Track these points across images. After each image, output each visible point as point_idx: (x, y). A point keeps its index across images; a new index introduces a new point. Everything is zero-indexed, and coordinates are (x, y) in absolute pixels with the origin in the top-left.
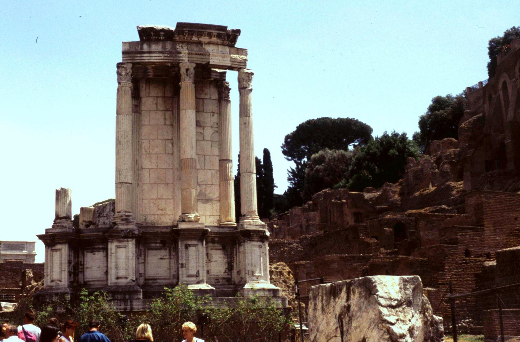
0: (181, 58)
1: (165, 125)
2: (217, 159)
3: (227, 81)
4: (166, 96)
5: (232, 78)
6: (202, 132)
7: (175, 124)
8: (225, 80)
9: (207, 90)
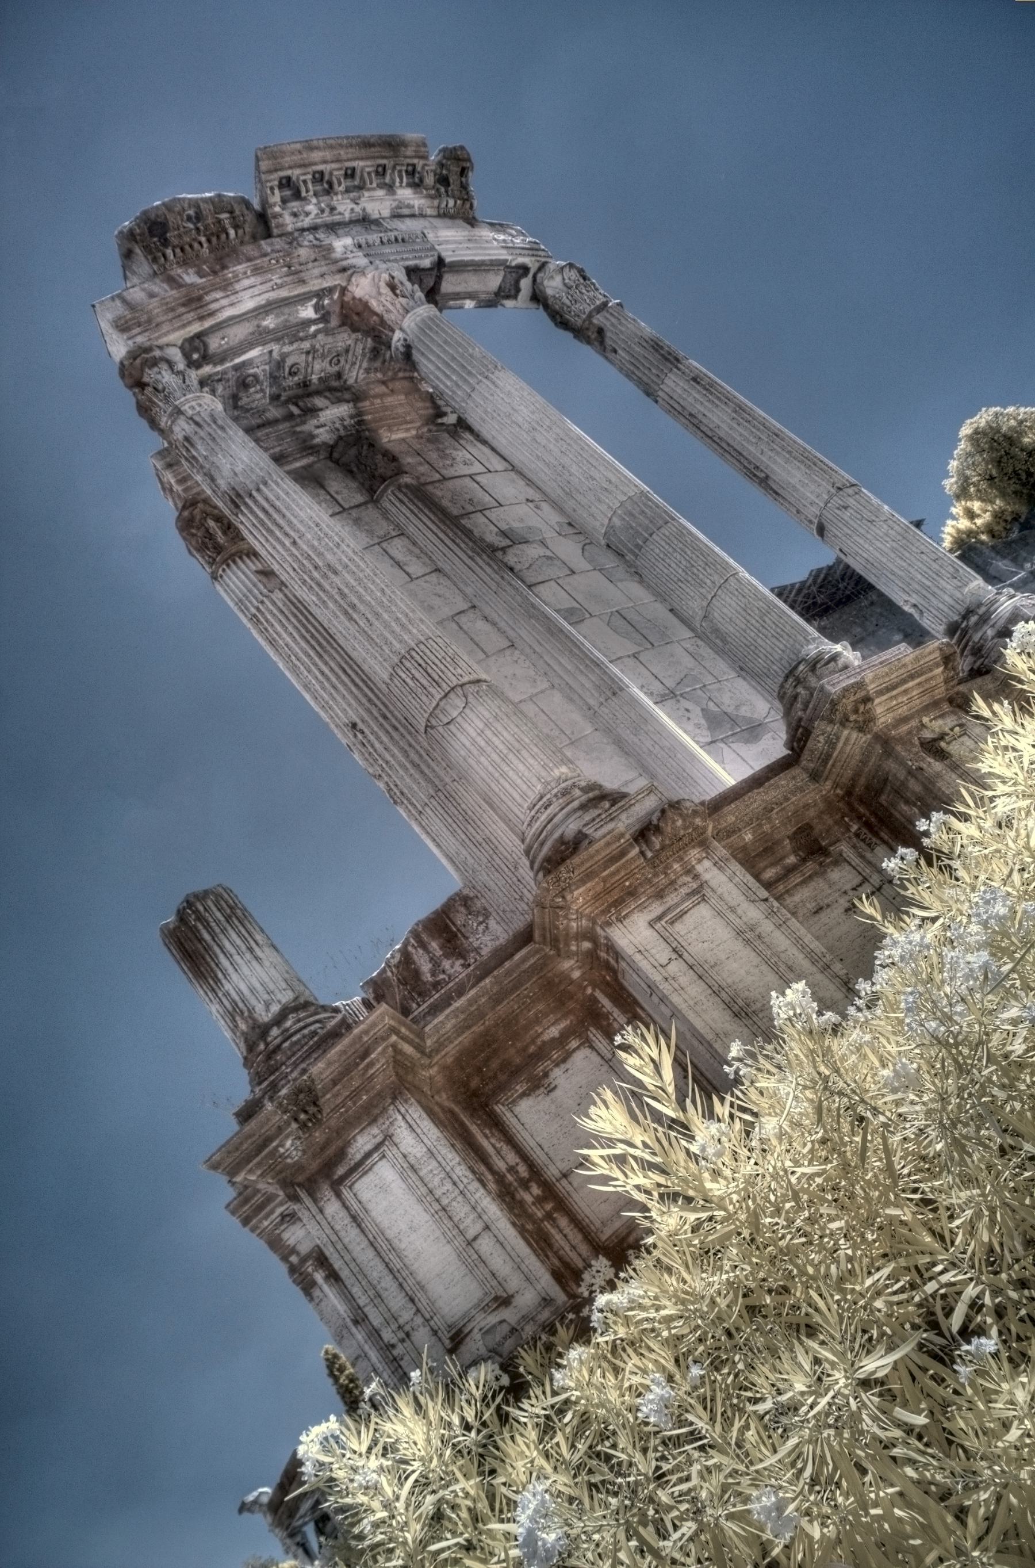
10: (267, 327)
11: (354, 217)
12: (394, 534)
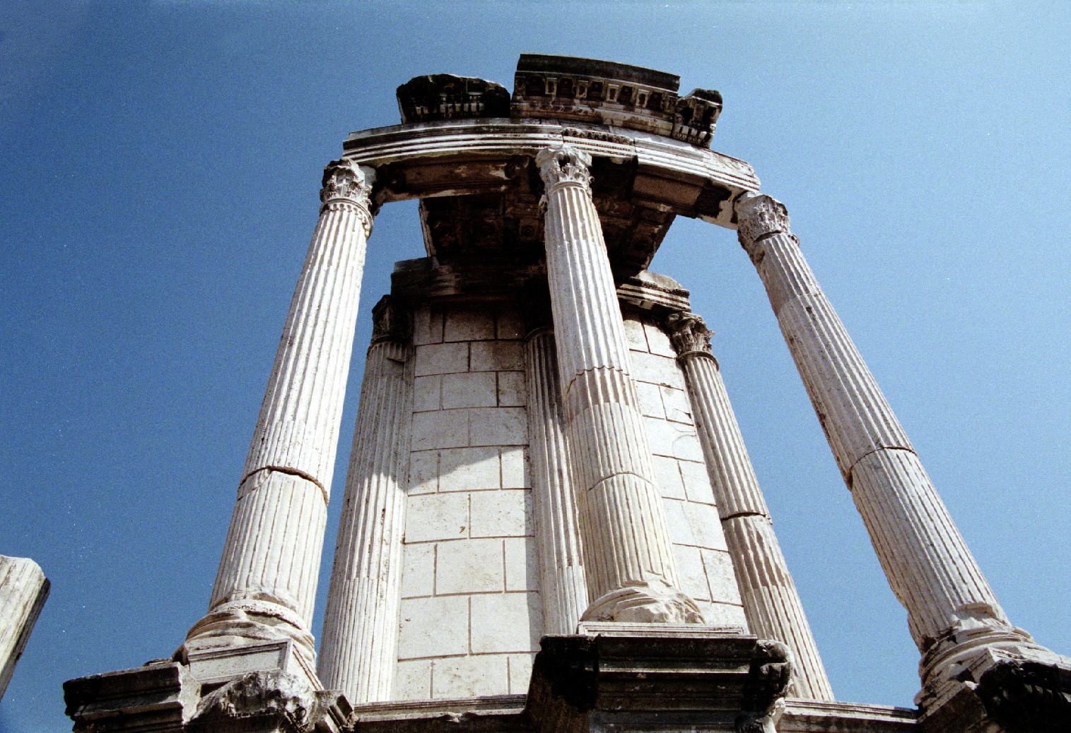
1: (498, 407)
2: (714, 514)
4: (499, 337)
10: (458, 176)
11: (587, 119)
12: (516, 368)
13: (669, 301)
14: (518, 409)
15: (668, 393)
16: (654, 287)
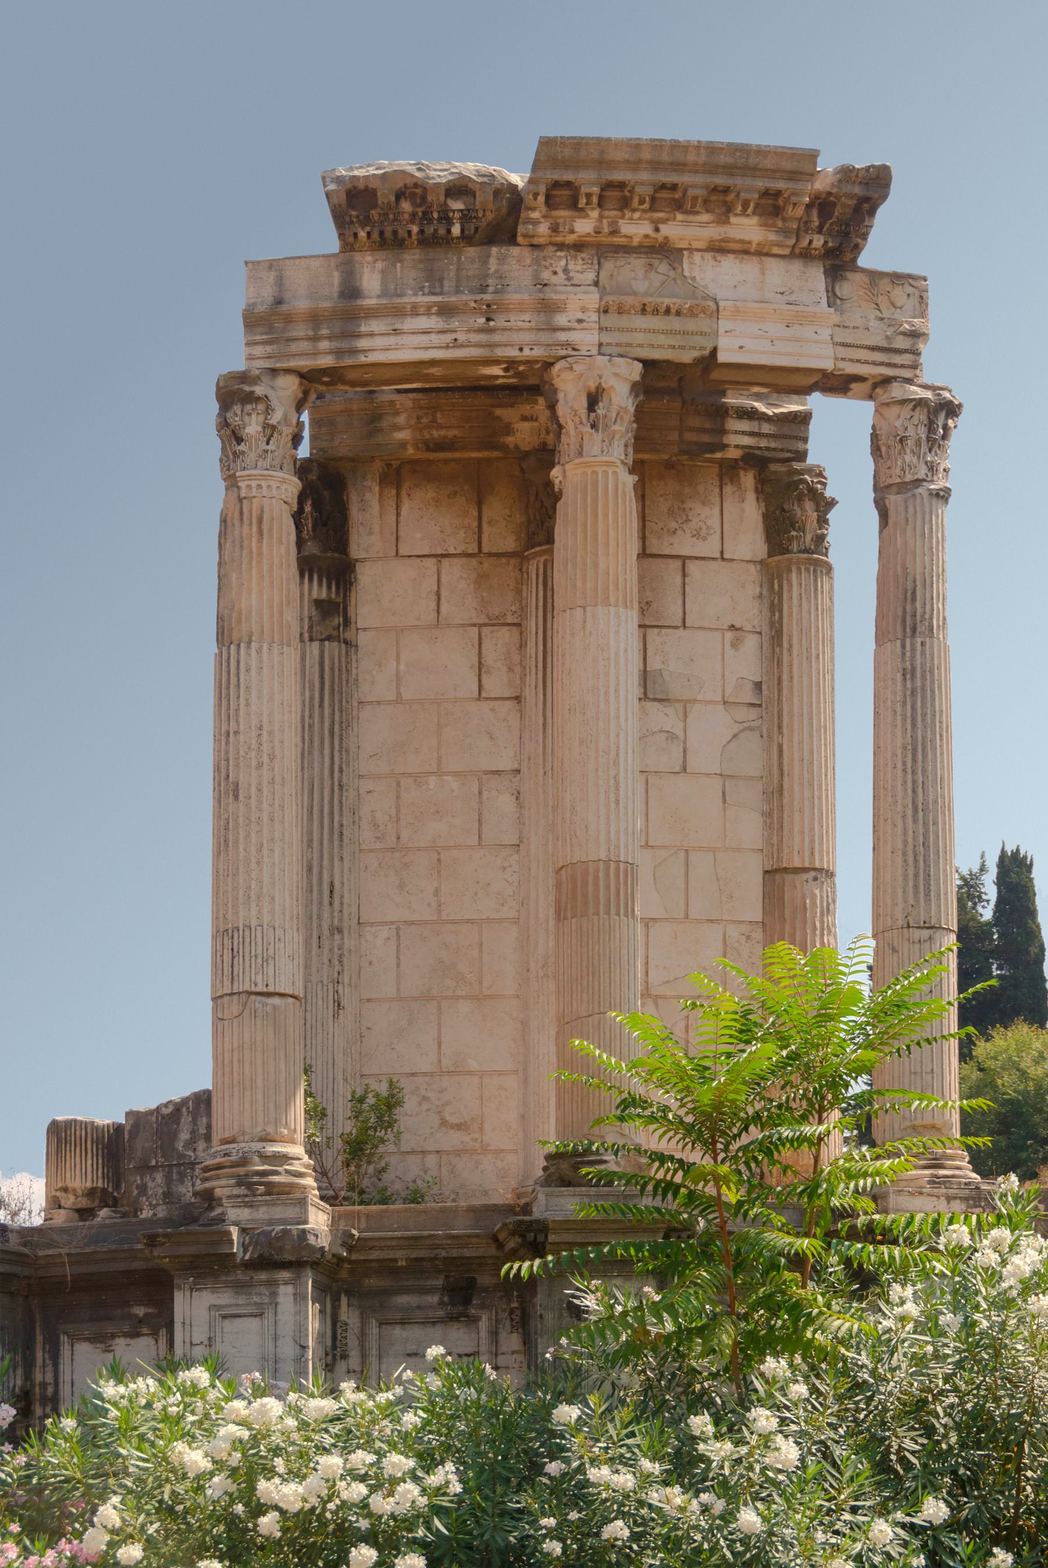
0: (562, 336)
3: (811, 460)
5: (839, 440)
6: (678, 731)
7: (529, 694)
8: (802, 456)
9: (705, 511)
13: (773, 445)
14: (508, 703)
15: (735, 644)
16: (752, 414)
